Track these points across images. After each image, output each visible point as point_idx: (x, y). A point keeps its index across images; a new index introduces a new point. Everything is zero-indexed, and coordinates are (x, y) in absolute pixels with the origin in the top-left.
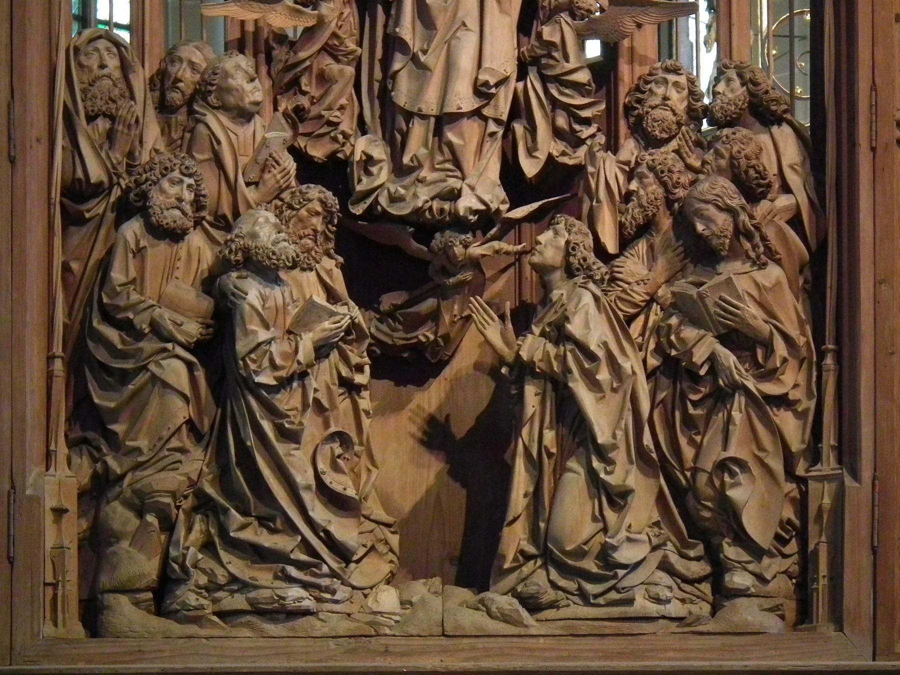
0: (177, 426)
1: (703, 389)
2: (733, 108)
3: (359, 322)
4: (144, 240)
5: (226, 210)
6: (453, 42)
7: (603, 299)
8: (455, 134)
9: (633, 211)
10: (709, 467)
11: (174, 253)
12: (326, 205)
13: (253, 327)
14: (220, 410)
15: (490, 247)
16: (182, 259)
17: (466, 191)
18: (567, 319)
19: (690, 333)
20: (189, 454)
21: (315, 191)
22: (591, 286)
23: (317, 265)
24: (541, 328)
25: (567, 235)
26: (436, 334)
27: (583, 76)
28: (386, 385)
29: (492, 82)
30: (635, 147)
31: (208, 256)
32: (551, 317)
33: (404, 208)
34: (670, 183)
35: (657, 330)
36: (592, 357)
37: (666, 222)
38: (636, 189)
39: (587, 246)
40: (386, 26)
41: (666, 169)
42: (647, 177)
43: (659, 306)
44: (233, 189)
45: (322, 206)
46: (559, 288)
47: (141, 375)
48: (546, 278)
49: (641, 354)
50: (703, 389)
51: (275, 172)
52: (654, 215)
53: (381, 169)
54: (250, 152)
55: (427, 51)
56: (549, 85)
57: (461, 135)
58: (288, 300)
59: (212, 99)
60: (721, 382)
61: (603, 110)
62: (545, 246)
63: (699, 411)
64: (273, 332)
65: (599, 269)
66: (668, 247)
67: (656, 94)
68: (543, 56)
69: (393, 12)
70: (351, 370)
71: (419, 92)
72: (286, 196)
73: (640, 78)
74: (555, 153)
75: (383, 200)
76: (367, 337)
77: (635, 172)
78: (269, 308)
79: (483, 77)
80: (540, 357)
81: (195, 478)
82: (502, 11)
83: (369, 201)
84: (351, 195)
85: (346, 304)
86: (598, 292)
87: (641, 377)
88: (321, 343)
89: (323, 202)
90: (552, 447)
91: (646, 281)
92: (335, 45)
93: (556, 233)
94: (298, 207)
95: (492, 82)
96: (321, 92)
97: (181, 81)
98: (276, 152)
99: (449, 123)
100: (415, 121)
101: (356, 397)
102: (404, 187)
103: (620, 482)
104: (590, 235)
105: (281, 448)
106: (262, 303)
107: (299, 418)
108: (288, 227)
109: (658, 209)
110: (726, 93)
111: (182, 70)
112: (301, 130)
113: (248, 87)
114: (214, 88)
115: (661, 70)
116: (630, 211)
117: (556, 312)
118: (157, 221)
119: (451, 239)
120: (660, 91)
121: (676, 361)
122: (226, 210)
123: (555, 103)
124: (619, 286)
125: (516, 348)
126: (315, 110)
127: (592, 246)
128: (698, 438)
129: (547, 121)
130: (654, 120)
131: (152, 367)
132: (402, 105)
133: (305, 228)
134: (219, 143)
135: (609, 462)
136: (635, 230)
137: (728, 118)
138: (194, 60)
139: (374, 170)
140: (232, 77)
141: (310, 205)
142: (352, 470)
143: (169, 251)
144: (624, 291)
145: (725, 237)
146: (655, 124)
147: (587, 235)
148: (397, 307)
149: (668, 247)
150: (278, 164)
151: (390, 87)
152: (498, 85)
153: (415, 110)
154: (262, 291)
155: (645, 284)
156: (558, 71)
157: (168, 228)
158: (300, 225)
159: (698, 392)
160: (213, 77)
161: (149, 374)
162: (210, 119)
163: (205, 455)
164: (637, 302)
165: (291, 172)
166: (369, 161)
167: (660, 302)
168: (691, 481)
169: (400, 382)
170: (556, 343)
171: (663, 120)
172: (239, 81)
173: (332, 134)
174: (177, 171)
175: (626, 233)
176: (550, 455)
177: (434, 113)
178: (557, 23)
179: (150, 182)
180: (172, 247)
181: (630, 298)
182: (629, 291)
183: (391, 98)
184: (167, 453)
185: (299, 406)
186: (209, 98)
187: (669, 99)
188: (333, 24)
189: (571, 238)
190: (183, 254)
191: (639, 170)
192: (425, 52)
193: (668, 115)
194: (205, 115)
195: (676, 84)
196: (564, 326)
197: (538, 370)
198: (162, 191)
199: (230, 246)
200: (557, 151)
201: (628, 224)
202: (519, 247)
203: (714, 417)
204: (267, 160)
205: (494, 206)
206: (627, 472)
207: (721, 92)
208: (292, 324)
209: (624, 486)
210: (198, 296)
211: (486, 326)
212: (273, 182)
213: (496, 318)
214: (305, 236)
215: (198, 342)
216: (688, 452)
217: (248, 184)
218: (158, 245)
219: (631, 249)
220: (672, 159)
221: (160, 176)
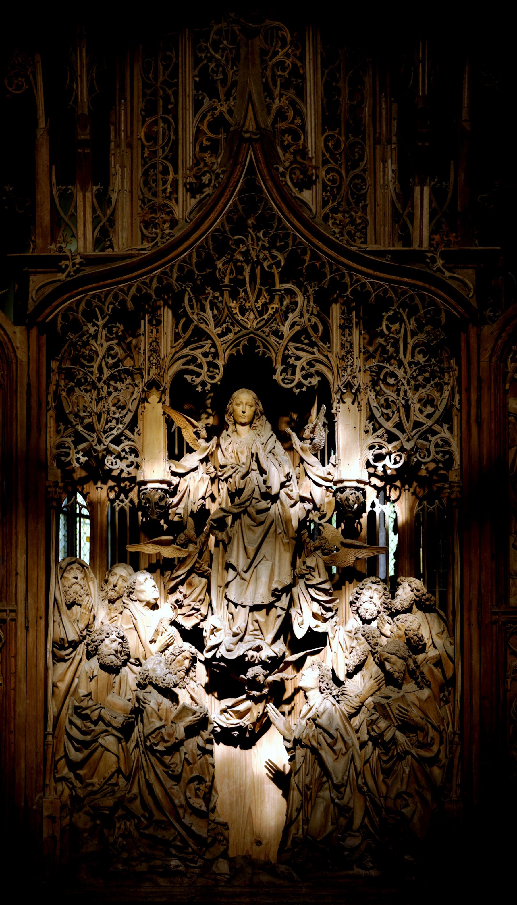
13: (153, 720)
33: (232, 655)
68: (307, 574)
69: (228, 550)
84: (205, 647)
148: (229, 707)
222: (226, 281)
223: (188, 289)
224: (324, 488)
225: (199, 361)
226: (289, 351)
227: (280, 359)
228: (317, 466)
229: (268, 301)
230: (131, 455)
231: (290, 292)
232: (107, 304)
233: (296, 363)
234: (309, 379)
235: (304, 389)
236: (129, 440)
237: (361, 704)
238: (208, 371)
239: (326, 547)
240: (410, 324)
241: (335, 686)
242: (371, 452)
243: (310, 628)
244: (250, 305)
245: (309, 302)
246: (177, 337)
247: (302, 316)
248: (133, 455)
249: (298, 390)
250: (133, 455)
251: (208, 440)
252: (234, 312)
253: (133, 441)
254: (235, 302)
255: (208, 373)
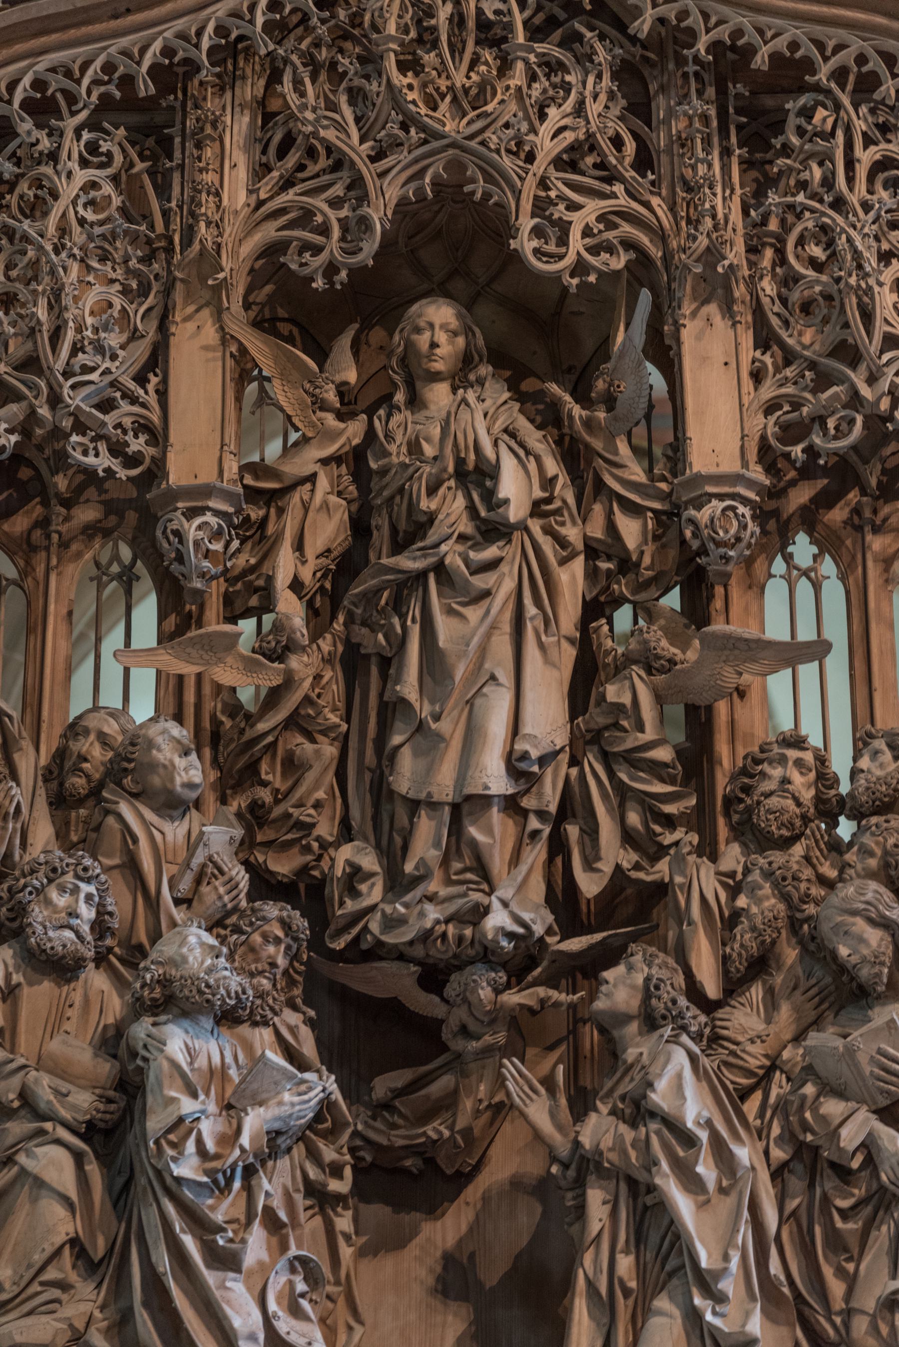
0: (57, 1246)
1: (856, 1191)
2: (884, 788)
3: (336, 1100)
4: (17, 973)
5: (142, 936)
6: (478, 701)
7: (705, 1061)
8: (481, 830)
9: (742, 936)
10: (870, 1305)
11: (64, 995)
12: (290, 928)
14: (123, 1225)
15: (533, 993)
16: (77, 1004)
17: (496, 904)
18: (650, 1085)
19: (833, 1108)
20: (72, 1292)
21: (272, 910)
22: (685, 1038)
23: (276, 1019)
24: (610, 1106)
25: (646, 969)
26: (451, 1128)
27: (663, 754)
28: (377, 1212)
29: (534, 754)
30: (742, 853)
31: (116, 1006)
32: (626, 1087)
34: (795, 896)
35: (782, 1107)
36: (689, 1140)
37: (790, 954)
38: (745, 906)
39: (676, 985)
40: (381, 695)
41: (789, 875)
42: (761, 888)
43: (784, 1076)
44: (153, 904)
45: (283, 929)
46: (637, 1045)
47: (5, 1171)
48: (616, 1033)
49: (761, 1146)
50: (856, 1191)
51: (217, 883)
52: (774, 942)
53: (373, 885)
54: (182, 855)
55: (442, 713)
56: (615, 767)
57: (489, 832)
58: (229, 1059)
59: (127, 781)
60: (884, 1177)
61: (694, 807)
62: (615, 986)
63: (850, 1226)
64: (203, 1103)
65: (694, 1017)
66: (795, 988)
67: (770, 778)
69: (392, 671)
70: (324, 1172)
71: (430, 770)
72: (234, 919)
73: (745, 757)
74: (626, 865)
75: (375, 926)
76: (346, 1124)
77: (744, 884)
78: (199, 1069)
79: (521, 746)
80: (610, 1145)
81: (80, 1325)
82: (547, 661)
83: (355, 931)
85: (318, 1071)
86: (696, 1049)
87: (764, 1176)
88: (277, 1125)
89: (286, 925)
90: (631, 1280)
91: (764, 1038)
92: (309, 715)
93: (630, 968)
94: (249, 929)
95: (534, 754)
96: (290, 783)
97: (86, 760)
98: (218, 854)
99: (470, 814)
100: (423, 812)
101: (331, 1213)
102: (406, 906)
103: (736, 1329)
104: (680, 972)
105: (210, 1277)
106: (189, 1059)
107: (241, 1235)
108: (234, 961)
109: (780, 933)
110: (874, 770)
111: (87, 744)
112: (259, 838)
113: (180, 762)
114: (133, 765)
115: (776, 745)
116: (738, 937)
117: (632, 1079)
118: (38, 945)
119: (475, 977)
120: (777, 772)
121: (815, 1150)
122: (142, 936)
123: (623, 791)
124: (726, 1048)
125: (574, 1134)
126: (277, 811)
127: (684, 987)
128: (851, 1267)
129: (613, 818)
130: (770, 811)
131: (22, 1158)
132: (404, 791)
133: (257, 960)
134: (135, 840)
135: (719, 1298)
136: (746, 964)
137: (877, 803)
138: (106, 730)
139: (363, 888)
140: (159, 750)
141: (266, 928)
142: (322, 1321)
143: (57, 991)
144: (733, 1053)
145: (882, 964)
146: (771, 817)
147: (676, 970)
149: (795, 988)
150: (222, 873)
151: (387, 772)
152: (542, 761)
153: (423, 796)
154: (191, 1045)
155: (763, 1042)
156: (629, 744)
157: (53, 955)
158: (251, 957)
159: (847, 1195)
160: (130, 749)
161: (15, 1169)
162: (125, 809)
163: (98, 1294)
164: (752, 1067)
165: (241, 885)
166: (355, 874)
167: (785, 1069)
168: (843, 1332)
169: (399, 1205)
170: (634, 1125)
171: (782, 811)
172: (165, 753)
173: (304, 842)
174: (72, 873)
175: (733, 969)
176: (627, 1292)
177: (450, 799)
178: (626, 678)
179: (29, 889)
180: (60, 987)
181: (741, 1063)
182: (739, 1052)
183: (389, 784)
184: (39, 1289)
185: (243, 1218)
186: (125, 781)
187: (789, 783)
188: (307, 684)
189: (654, 971)
190: (77, 998)
191: (749, 879)
192: (437, 718)
193: (790, 803)
194: (117, 803)
195: (799, 763)
196: (645, 1096)
197: (606, 1165)
198: (48, 902)
199: (143, 977)
200: (629, 861)
201: (735, 955)
202: (576, 997)
203: (874, 1233)
204: (204, 866)
205: (539, 930)
206: (747, 1315)
207: (865, 768)
208: (234, 1093)
209: (743, 1333)
210: (96, 1055)
211: (528, 1101)
212: (214, 896)
213: (542, 1090)
214: (261, 973)
215: (90, 1124)
216: (837, 1288)
217: (178, 902)
218: (40, 983)
219: (740, 996)
220: (798, 862)
221: (45, 881)
222: (392, 28)
223: (294, 58)
224: (650, 514)
225: (319, 219)
226: (550, 189)
227: (527, 205)
228: (629, 464)
229: (495, 73)
230: (136, 436)
231: (552, 67)
232: (86, 82)
233: (569, 216)
234: (604, 256)
235: (592, 278)
236: (134, 400)
237: (767, 1063)
238: (343, 239)
239: (659, 651)
240: (859, 118)
241: (694, 1011)
242: (772, 419)
243: (618, 867)
244: (449, 83)
245: (599, 76)
246: (261, 171)
247: (580, 110)
248: (142, 439)
249: (575, 281)
250: (142, 439)
251: (341, 416)
252: (410, 98)
253: (144, 405)
254: (410, 74)
255: (343, 245)
